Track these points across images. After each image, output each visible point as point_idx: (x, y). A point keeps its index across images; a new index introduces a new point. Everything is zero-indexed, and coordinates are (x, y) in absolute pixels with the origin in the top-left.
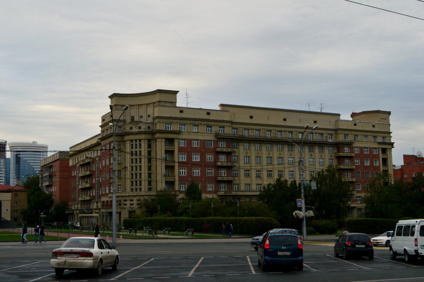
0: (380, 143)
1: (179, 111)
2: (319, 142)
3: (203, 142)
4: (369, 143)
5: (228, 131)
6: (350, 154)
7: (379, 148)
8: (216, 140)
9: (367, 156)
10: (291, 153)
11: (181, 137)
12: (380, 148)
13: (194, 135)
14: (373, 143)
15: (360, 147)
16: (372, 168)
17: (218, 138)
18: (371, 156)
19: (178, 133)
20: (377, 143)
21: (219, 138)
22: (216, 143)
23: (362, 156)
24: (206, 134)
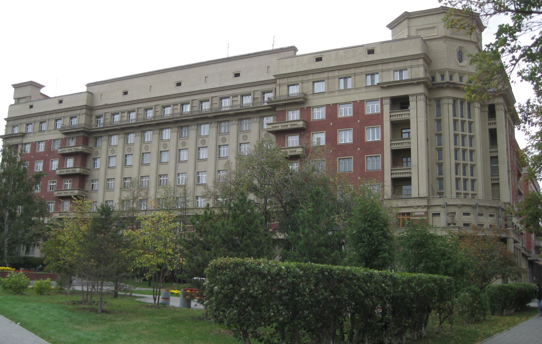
0: (384, 86)
1: (29, 107)
2: (233, 112)
3: (49, 143)
4: (353, 91)
5: (79, 121)
6: (282, 124)
7: (382, 99)
8: (63, 136)
9: (346, 123)
10: (184, 140)
11: (25, 140)
12: (385, 98)
13: (40, 135)
14: (363, 90)
15: (328, 106)
16: (359, 149)
17: (65, 134)
18: (359, 121)
19: (23, 135)
20: (379, 88)
21: (68, 133)
22: (64, 143)
23: (331, 124)
24: (52, 132)
